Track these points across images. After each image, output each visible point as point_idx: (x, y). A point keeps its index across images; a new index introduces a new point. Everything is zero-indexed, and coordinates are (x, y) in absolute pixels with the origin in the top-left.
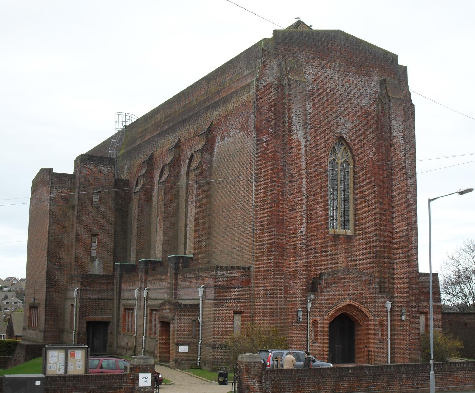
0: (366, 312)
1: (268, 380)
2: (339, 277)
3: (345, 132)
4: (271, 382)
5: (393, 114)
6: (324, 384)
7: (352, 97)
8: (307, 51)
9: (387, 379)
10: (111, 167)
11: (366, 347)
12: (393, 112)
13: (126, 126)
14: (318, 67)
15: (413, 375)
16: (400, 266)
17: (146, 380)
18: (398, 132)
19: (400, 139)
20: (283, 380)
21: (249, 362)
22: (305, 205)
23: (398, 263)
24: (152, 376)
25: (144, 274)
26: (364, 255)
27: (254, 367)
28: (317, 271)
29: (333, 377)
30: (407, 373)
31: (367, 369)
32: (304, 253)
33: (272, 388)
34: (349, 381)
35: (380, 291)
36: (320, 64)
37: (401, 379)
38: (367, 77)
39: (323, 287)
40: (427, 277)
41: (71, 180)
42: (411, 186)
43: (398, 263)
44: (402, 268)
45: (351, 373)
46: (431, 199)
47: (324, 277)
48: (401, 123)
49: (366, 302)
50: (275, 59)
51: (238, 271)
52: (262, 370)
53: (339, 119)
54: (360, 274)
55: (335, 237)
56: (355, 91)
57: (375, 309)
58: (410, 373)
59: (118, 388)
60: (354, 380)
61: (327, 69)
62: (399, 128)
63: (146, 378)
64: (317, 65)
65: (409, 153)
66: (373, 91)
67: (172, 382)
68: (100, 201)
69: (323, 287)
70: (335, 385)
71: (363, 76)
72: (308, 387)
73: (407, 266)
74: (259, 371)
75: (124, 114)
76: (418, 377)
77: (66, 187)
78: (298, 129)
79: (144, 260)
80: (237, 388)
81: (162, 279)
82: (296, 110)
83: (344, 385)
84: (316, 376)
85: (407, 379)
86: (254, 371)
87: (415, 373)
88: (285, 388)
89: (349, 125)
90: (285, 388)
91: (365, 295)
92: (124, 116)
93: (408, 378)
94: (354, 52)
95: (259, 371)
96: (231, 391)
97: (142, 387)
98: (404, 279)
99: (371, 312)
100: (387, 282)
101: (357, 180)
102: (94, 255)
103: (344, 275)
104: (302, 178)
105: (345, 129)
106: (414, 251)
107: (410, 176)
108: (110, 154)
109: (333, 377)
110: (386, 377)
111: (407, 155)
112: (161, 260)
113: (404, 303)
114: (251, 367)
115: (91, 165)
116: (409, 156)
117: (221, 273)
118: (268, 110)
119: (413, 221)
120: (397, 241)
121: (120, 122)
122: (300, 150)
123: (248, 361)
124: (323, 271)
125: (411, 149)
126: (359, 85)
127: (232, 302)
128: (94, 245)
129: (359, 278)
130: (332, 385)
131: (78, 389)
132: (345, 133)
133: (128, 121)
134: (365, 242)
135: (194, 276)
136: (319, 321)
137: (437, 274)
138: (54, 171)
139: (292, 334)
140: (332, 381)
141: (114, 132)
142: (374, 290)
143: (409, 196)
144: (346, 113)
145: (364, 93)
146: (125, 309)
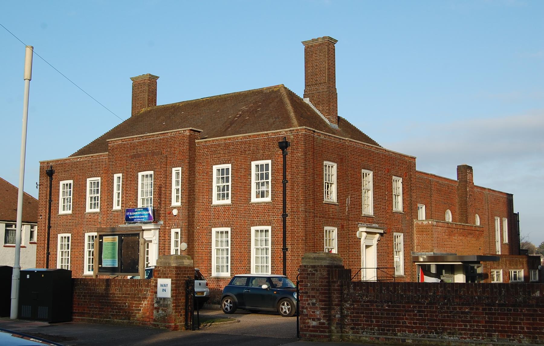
1: (346, 302)
4: (353, 305)
6: (466, 317)
17: (164, 288)
20: (376, 302)
21: (305, 266)
27: (314, 274)
33: (354, 317)
34: (532, 315)
45: (537, 298)
59: (142, 298)
70: (495, 322)
74: (322, 282)
83: (520, 323)
84: (449, 300)
86: (314, 282)
88: (381, 318)
90: (381, 318)
95: (322, 282)
97: (161, 298)
114: (308, 274)
123: (305, 264)
130: (486, 322)
140: (486, 314)
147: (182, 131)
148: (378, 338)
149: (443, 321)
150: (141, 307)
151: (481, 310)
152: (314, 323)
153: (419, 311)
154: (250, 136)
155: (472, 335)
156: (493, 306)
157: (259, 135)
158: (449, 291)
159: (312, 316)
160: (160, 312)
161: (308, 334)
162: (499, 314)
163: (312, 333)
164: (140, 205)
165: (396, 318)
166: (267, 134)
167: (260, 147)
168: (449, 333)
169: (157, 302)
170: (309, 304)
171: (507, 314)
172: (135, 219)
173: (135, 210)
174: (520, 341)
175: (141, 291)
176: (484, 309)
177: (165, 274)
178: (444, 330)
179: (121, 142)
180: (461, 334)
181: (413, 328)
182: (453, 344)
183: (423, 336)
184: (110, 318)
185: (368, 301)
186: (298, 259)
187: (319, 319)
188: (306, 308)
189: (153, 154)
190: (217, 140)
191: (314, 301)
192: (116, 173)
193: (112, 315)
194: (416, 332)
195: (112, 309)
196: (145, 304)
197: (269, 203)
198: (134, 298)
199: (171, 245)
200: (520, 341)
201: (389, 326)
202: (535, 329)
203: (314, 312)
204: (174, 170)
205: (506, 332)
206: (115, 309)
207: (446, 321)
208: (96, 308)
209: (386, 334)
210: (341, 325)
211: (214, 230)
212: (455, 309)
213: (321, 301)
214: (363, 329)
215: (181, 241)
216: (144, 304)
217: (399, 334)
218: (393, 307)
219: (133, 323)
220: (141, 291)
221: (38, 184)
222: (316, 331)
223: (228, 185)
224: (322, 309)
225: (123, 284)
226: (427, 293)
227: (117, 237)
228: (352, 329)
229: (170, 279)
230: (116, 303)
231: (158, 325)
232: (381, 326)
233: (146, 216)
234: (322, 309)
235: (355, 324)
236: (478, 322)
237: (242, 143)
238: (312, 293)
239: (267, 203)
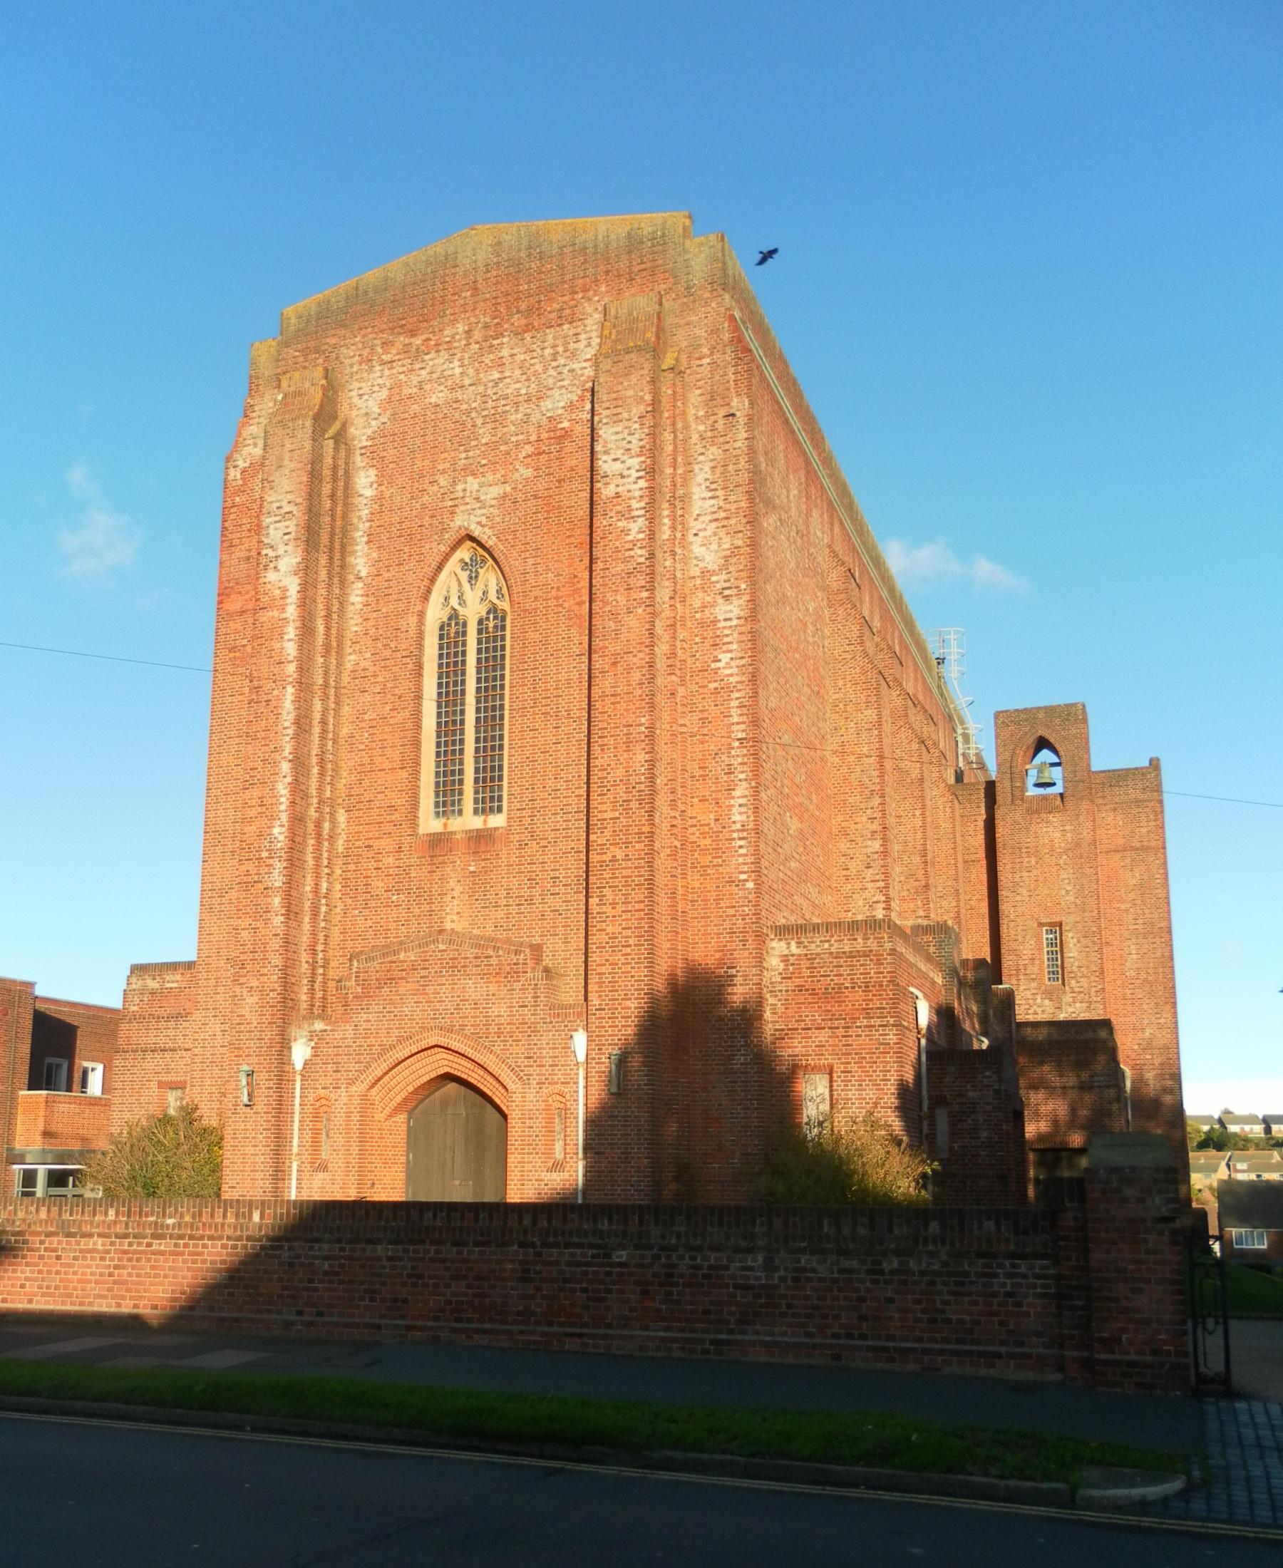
2: (405, 961)
3: (478, 519)
5: (607, 405)
7: (507, 408)
12: (605, 399)
14: (399, 360)
16: (614, 905)
18: (625, 458)
19: (632, 479)
22: (290, 761)
23: (607, 891)
26: (537, 883)
32: (277, 901)
39: (351, 996)
40: (836, 937)
42: (729, 624)
43: (607, 891)
48: (637, 426)
49: (499, 1034)
51: (182, 974)
53: (460, 487)
54: (478, 946)
55: (438, 842)
56: (518, 385)
57: (530, 1058)
61: (427, 357)
62: (630, 442)
64: (397, 358)
65: (723, 515)
66: (586, 361)
69: (351, 996)
71: (548, 331)
73: (643, 902)
78: (281, 552)
82: (278, 504)
89: (495, 491)
91: (494, 1011)
98: (630, 946)
103: (423, 952)
105: (480, 508)
106: (741, 847)
116: (723, 526)
117: (140, 983)
118: (250, 530)
119: (736, 744)
120: (605, 820)
122: (283, 610)
125: (732, 498)
126: (532, 361)
129: (476, 958)
132: (479, 523)
134: (538, 843)
136: (336, 1100)
139: (233, 1138)
143: (720, 661)
144: (484, 462)
145: (551, 381)
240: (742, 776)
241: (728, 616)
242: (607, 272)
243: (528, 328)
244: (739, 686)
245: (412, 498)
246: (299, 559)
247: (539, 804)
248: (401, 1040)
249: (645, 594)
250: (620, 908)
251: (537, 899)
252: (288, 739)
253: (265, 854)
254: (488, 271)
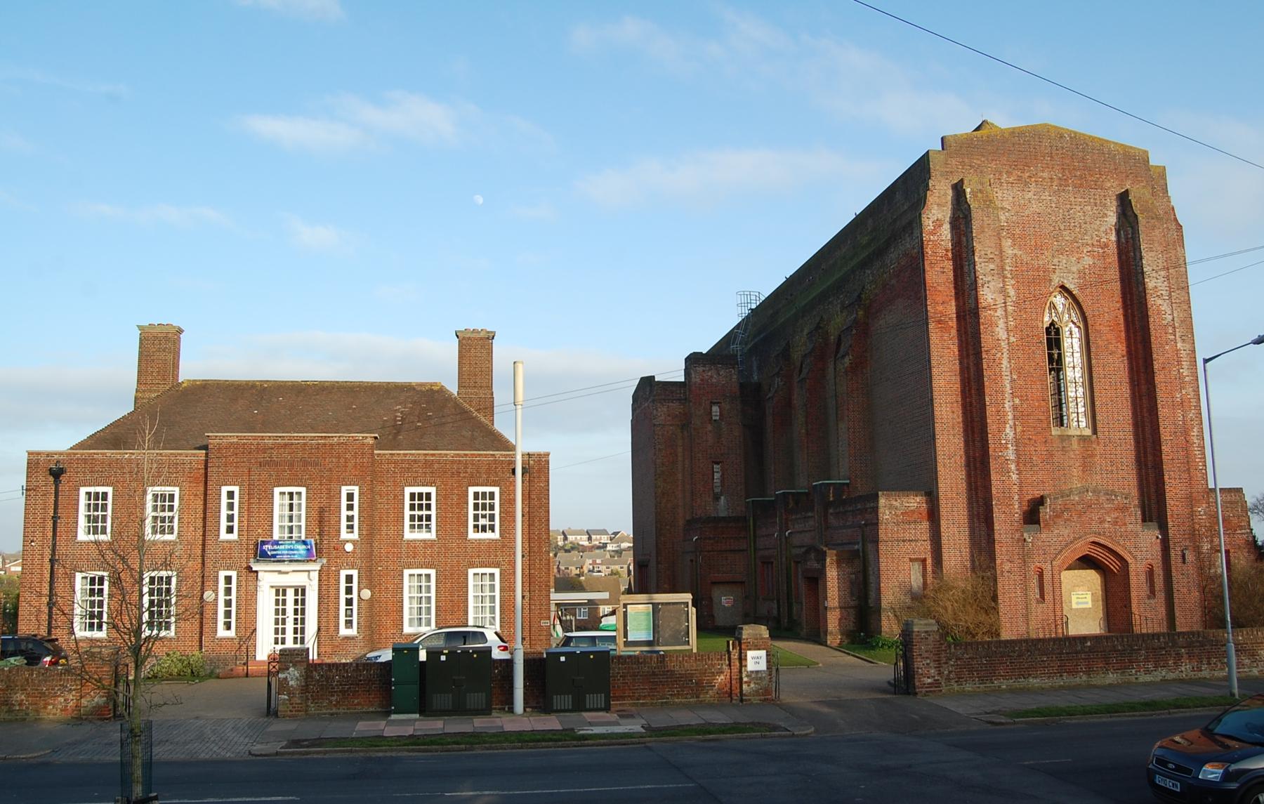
0: (1121, 553)
1: (951, 660)
4: (956, 662)
6: (1044, 664)
8: (998, 162)
9: (1153, 655)
10: (733, 368)
11: (1125, 607)
13: (752, 309)
15: (1200, 650)
16: (1175, 479)
21: (918, 632)
23: (1172, 473)
24: (767, 655)
25: (783, 511)
27: (927, 638)
28: (1038, 492)
29: (1059, 654)
30: (1189, 646)
31: (1118, 639)
32: (1013, 467)
34: (1087, 659)
35: (1144, 520)
36: (1019, 178)
37: (1179, 656)
38: (1099, 190)
41: (680, 390)
43: (1172, 473)
44: (1178, 481)
45: (1089, 647)
46: (1207, 358)
47: (1049, 501)
49: (1121, 536)
50: (947, 179)
52: (941, 644)
54: (1108, 494)
58: (1195, 647)
59: (717, 673)
60: (1096, 658)
63: (758, 658)
64: (1015, 182)
67: (818, 664)
68: (721, 415)
70: (1064, 666)
72: (1018, 669)
74: (934, 645)
75: (748, 293)
76: (1209, 652)
77: (675, 400)
79: (782, 491)
80: (902, 672)
81: (809, 517)
84: (1031, 653)
85: (1190, 656)
86: (928, 645)
87: (1202, 646)
88: (981, 671)
92: (749, 296)
93: (1190, 656)
94: (1073, 155)
96: (893, 677)
97: (752, 672)
99: (1130, 552)
100: (1153, 506)
101: (1093, 349)
102: (717, 490)
104: (1002, 354)
107: (1183, 337)
108: (733, 350)
109: (1059, 654)
110: (1151, 652)
111: (1174, 305)
112: (807, 491)
113: (1186, 536)
114: (922, 639)
115: (704, 366)
118: (942, 257)
119: (1193, 408)
121: (743, 305)
124: (1047, 493)
127: (907, 544)
128: (717, 476)
131: (657, 675)
133: (755, 302)
135: (850, 509)
137: (1242, 489)
138: (656, 380)
141: (736, 320)
142: (1133, 518)
144: (1068, 249)
146: (763, 563)
147: (361, 438)
148: (979, 687)
149: (1029, 668)
150: (715, 683)
151: (1054, 658)
152: (929, 681)
153: (1010, 663)
154: (466, 455)
155: (1049, 677)
156: (1063, 654)
157: (480, 455)
158: (1030, 646)
159: (926, 674)
160: (752, 685)
161: (924, 690)
162: (1067, 660)
163: (928, 689)
164: (276, 537)
165: (992, 670)
166: (494, 455)
167: (483, 470)
168: (1033, 677)
169: (747, 676)
170: (923, 665)
171: (1071, 660)
172: (278, 555)
173: (280, 542)
174: (1081, 678)
175: (713, 665)
176: (1057, 657)
177: (756, 646)
178: (1030, 675)
179: (236, 440)
180: (1041, 677)
181: (1006, 676)
182: (1036, 685)
183: (1014, 682)
184: (668, 698)
185: (970, 658)
186: (540, 609)
187: (934, 677)
188: (921, 668)
189: (306, 464)
190: (411, 454)
191: (928, 661)
192: (226, 485)
193: (672, 695)
194: (1008, 679)
195: (670, 688)
196: (722, 679)
197: (496, 540)
198: (705, 673)
199: (341, 593)
200: (1081, 678)
201: (989, 676)
202: (1090, 668)
203: (928, 671)
204: (345, 490)
205: (1071, 672)
206: (676, 688)
207: (1031, 668)
208: (646, 689)
209: (985, 683)
210: (948, 679)
211: (407, 572)
212: (1036, 658)
213: (934, 661)
214: (966, 681)
215: (359, 587)
216: (720, 680)
217: (995, 682)
218: (990, 661)
219: (705, 700)
220: (713, 665)
221: (25, 488)
222: (931, 687)
223: (233, 492)
224: (935, 668)
225: (683, 659)
226: (1014, 648)
227: (651, 606)
228: (956, 682)
229: (765, 651)
230: (676, 681)
231: (750, 700)
232: (981, 677)
233: (303, 552)
234: (935, 668)
235: (959, 678)
236: (1053, 667)
237: (453, 462)
238: (925, 655)
239: (493, 540)
240: (1197, 423)
241: (1185, 348)
242: (1116, 169)
243: (1081, 186)
244: (1192, 382)
245: (1032, 259)
246: (1002, 285)
247: (1111, 426)
248: (1075, 539)
249: (1173, 337)
250: (1178, 481)
251: (1115, 472)
252: (1008, 381)
253: (1003, 442)
254: (1057, 150)
